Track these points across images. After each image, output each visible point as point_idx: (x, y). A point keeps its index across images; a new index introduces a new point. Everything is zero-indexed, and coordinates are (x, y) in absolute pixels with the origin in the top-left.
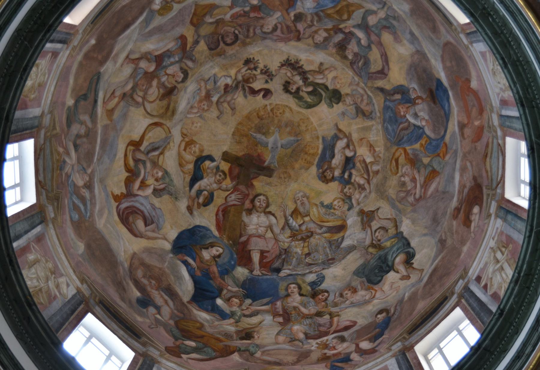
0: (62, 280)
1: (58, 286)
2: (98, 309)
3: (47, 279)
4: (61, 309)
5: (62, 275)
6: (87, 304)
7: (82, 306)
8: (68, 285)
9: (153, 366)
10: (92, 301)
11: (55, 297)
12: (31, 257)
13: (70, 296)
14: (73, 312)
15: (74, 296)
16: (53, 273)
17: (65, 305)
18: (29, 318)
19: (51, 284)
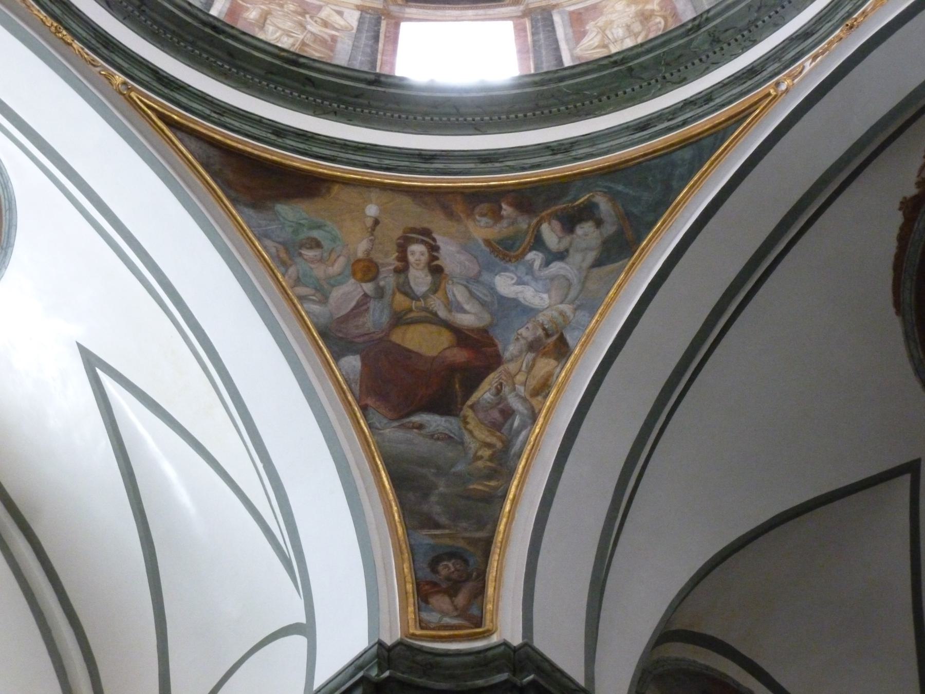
0: (323, 14)
1: (325, 24)
2: (411, 11)
3: (303, 26)
4: (355, 47)
5: (320, 8)
6: (389, 15)
7: (384, 24)
8: (340, 13)
9: (551, 16)
10: (393, 9)
11: (334, 39)
12: (253, 14)
13: (355, 24)
14: (376, 38)
15: (361, 21)
16: (303, 13)
17: (357, 38)
18: (310, 80)
19: (314, 28)
